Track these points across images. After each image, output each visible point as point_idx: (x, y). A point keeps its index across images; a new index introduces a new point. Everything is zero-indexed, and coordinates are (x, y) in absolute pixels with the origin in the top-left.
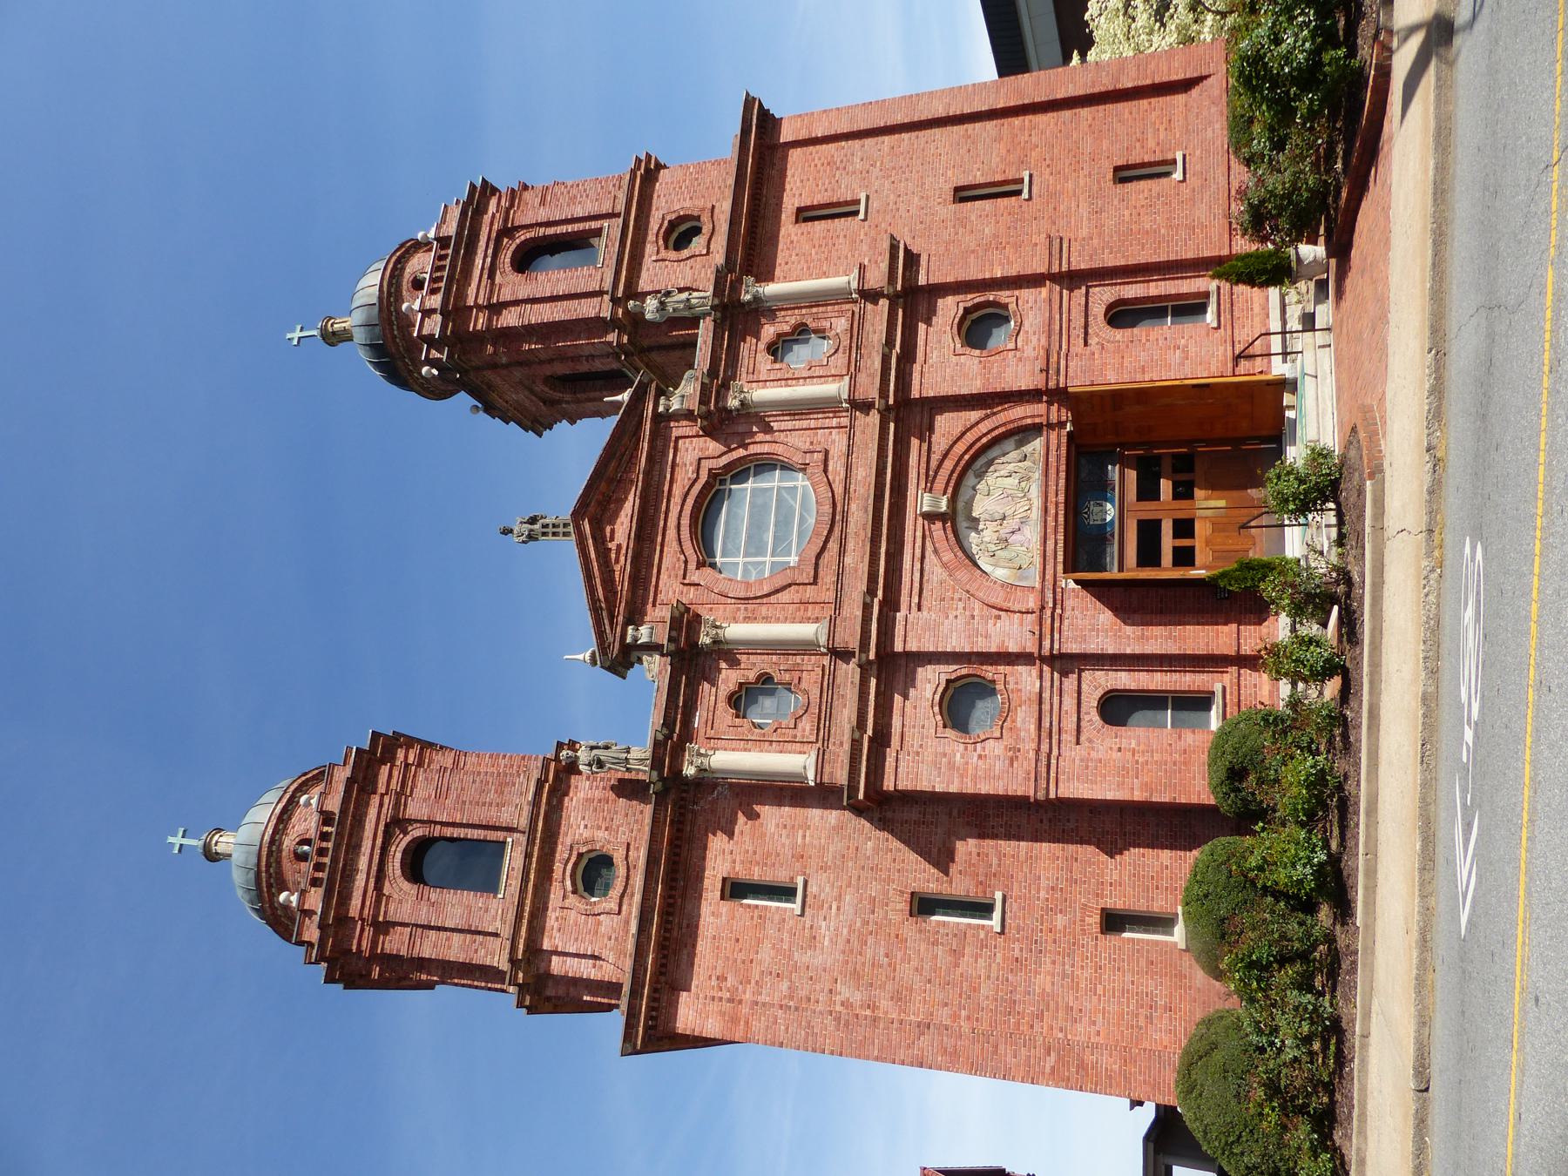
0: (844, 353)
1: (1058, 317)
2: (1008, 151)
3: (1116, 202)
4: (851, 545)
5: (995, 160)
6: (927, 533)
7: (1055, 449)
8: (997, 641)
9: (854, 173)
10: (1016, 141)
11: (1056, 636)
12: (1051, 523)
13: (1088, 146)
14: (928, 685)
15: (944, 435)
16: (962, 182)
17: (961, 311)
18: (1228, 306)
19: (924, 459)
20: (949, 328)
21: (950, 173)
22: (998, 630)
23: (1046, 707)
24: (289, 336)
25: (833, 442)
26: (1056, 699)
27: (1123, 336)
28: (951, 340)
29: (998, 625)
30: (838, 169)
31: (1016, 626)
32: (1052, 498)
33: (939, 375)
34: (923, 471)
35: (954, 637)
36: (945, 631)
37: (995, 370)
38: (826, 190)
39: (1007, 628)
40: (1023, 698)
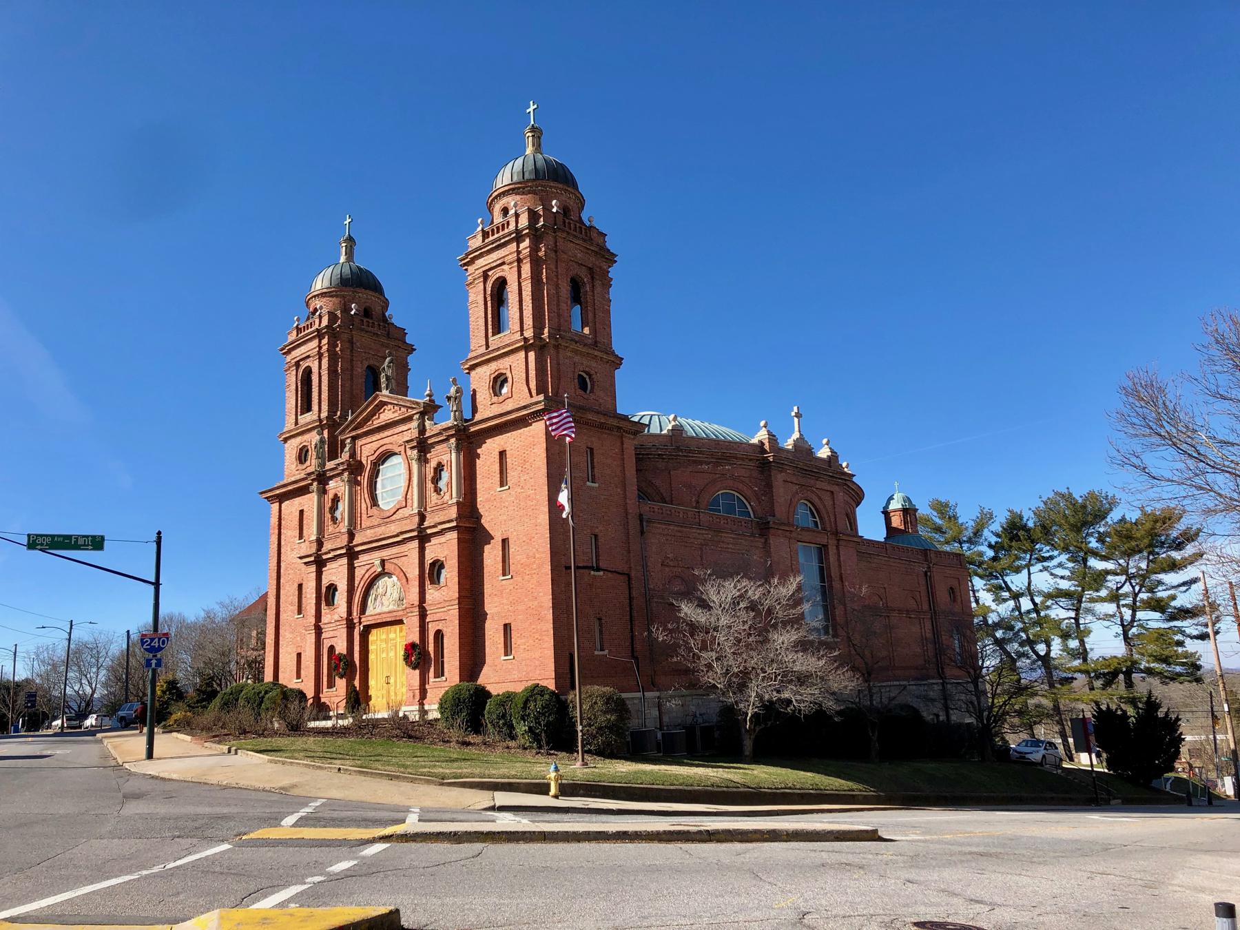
2: (522, 564)
3: (496, 626)
4: (372, 531)
5: (519, 558)
9: (520, 477)
10: (526, 567)
11: (340, 627)
13: (521, 607)
16: (511, 542)
18: (436, 686)
21: (515, 533)
23: (329, 625)
24: (528, 111)
26: (330, 629)
30: (522, 467)
34: (391, 557)
38: (513, 464)
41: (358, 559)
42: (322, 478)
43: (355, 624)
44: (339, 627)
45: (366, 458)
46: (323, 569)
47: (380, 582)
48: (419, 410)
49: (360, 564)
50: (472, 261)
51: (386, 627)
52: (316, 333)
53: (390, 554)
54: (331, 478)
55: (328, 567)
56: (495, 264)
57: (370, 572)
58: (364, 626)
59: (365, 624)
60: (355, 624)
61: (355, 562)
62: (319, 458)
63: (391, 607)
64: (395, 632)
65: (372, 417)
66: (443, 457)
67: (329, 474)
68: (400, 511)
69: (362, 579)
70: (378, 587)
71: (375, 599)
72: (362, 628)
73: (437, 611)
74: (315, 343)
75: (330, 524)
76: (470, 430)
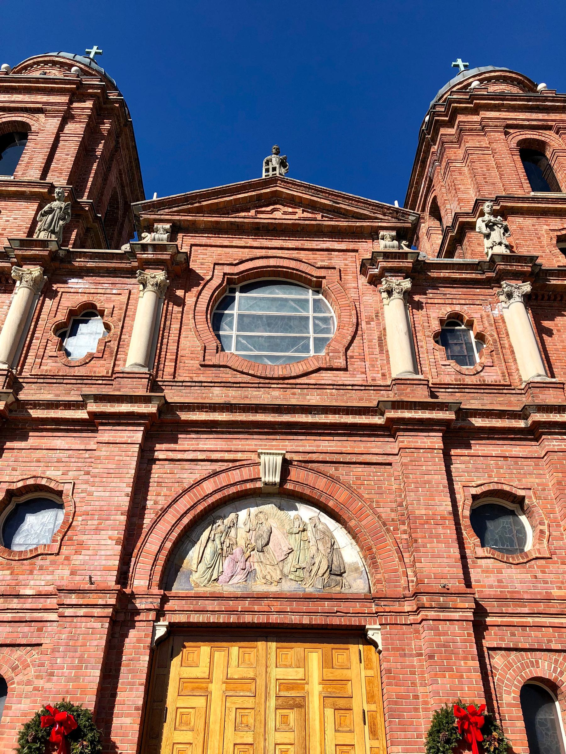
0: (456, 380)
1: (526, 610)
6: (238, 464)
7: (342, 609)
8: (90, 542)
11: (81, 612)
12: (240, 606)
14: (60, 473)
15: (358, 479)
17: (521, 493)
19: (328, 458)
20: (496, 480)
22: (103, 542)
25: (353, 375)
27: (509, 705)
28: (479, 482)
29: (109, 542)
31: (104, 562)
32: (276, 605)
33: (430, 468)
34: (314, 457)
35: (102, 494)
36: (113, 484)
37: (440, 530)
39: (103, 553)
40: (21, 577)
41: (175, 441)
42: (57, 264)
43: (137, 612)
44: (68, 612)
45: (212, 266)
46: (8, 444)
47: (243, 514)
48: (399, 225)
49: (171, 455)
50: (475, 111)
51: (261, 645)
52: (75, 86)
53: (308, 449)
54: (81, 273)
55: (34, 440)
56: (527, 123)
57: (222, 480)
58: (172, 628)
59: (181, 618)
60: (137, 612)
61: (158, 446)
62: (53, 232)
63: (288, 587)
64: (303, 663)
65: (238, 212)
66: (465, 307)
67: (79, 263)
68: (324, 374)
69: (185, 491)
70: (234, 524)
71: (220, 555)
72: (161, 632)
73: (530, 620)
74: (64, 99)
75: (49, 353)
76: (549, 280)
